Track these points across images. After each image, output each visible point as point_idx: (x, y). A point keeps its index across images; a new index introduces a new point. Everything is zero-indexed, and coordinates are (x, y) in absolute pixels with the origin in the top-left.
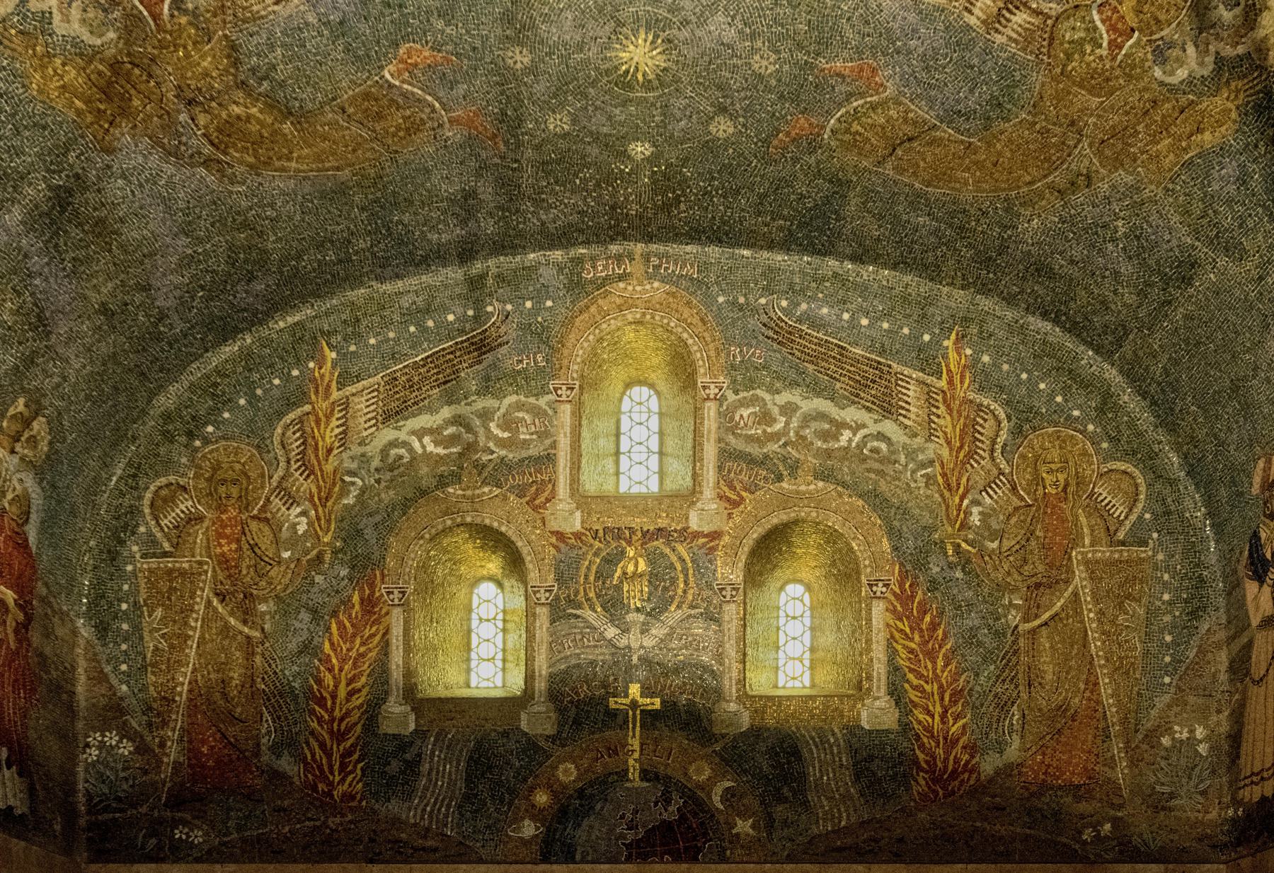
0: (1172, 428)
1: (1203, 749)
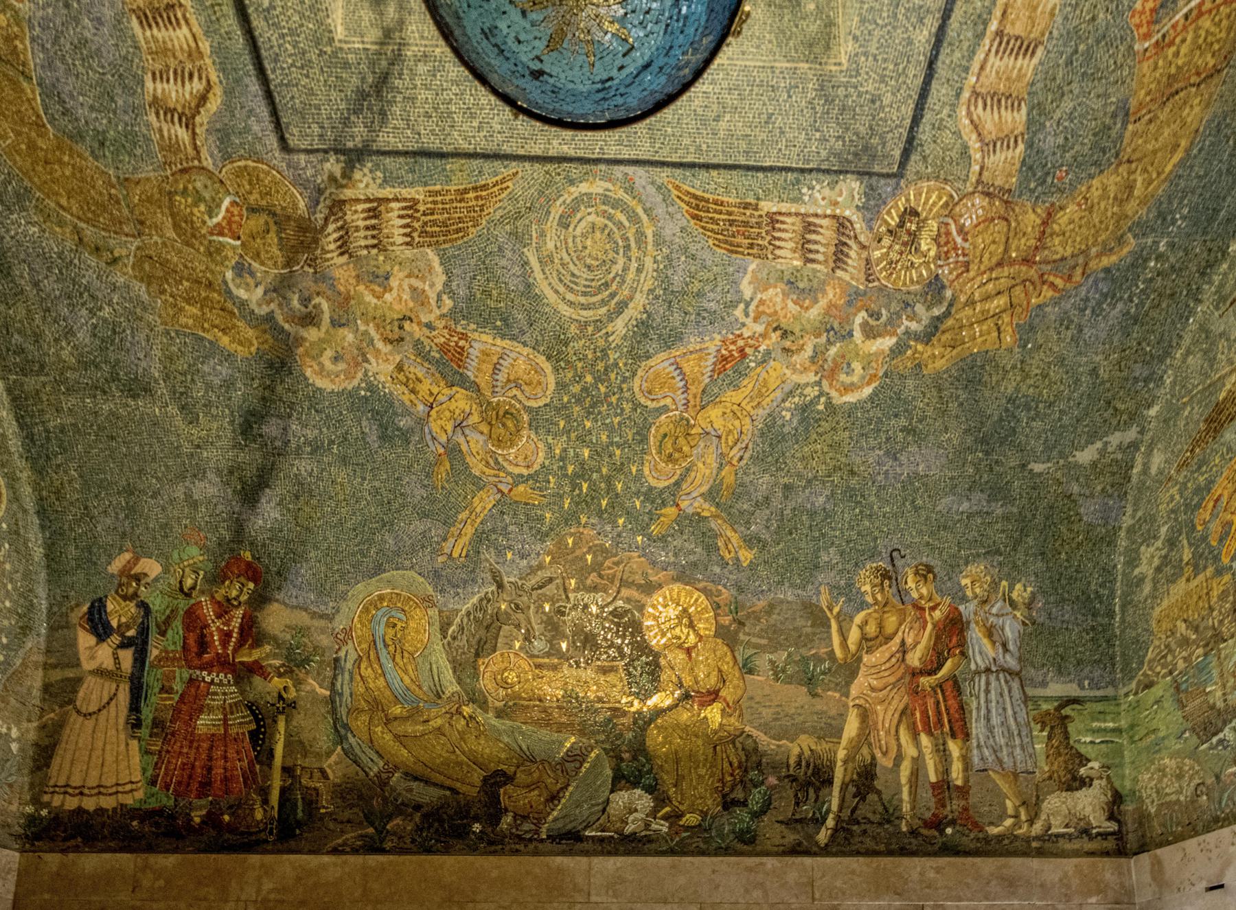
0: (40, 472)
1: (14, 747)
